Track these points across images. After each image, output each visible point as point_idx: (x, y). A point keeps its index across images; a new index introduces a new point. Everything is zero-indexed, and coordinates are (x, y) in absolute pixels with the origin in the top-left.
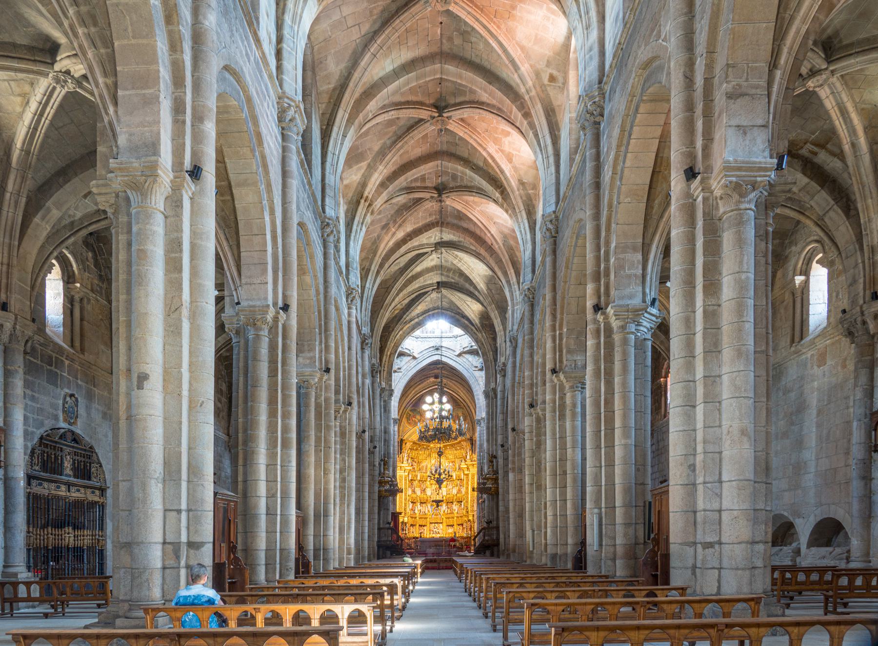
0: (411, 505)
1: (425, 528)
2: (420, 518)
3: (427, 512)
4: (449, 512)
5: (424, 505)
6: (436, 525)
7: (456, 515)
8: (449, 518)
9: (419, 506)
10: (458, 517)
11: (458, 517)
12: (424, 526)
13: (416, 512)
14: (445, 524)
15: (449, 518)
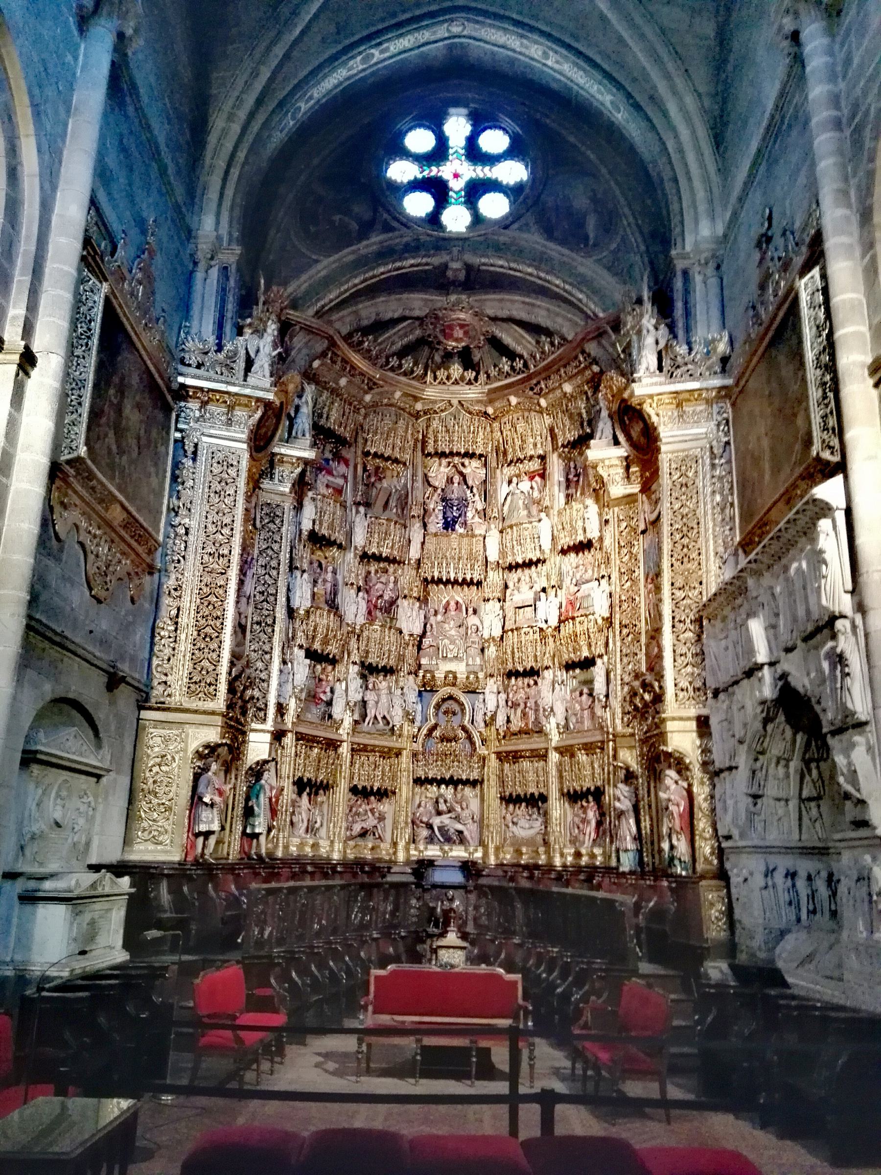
0: (301, 668)
1: (385, 807)
2: (355, 751)
3: (397, 718)
4: (517, 724)
5: (383, 683)
6: (447, 792)
7: (555, 739)
8: (515, 757)
9: (355, 683)
10: (566, 751)
11: (560, 750)
12: (383, 794)
13: (338, 710)
14: (492, 791)
15: (515, 757)
